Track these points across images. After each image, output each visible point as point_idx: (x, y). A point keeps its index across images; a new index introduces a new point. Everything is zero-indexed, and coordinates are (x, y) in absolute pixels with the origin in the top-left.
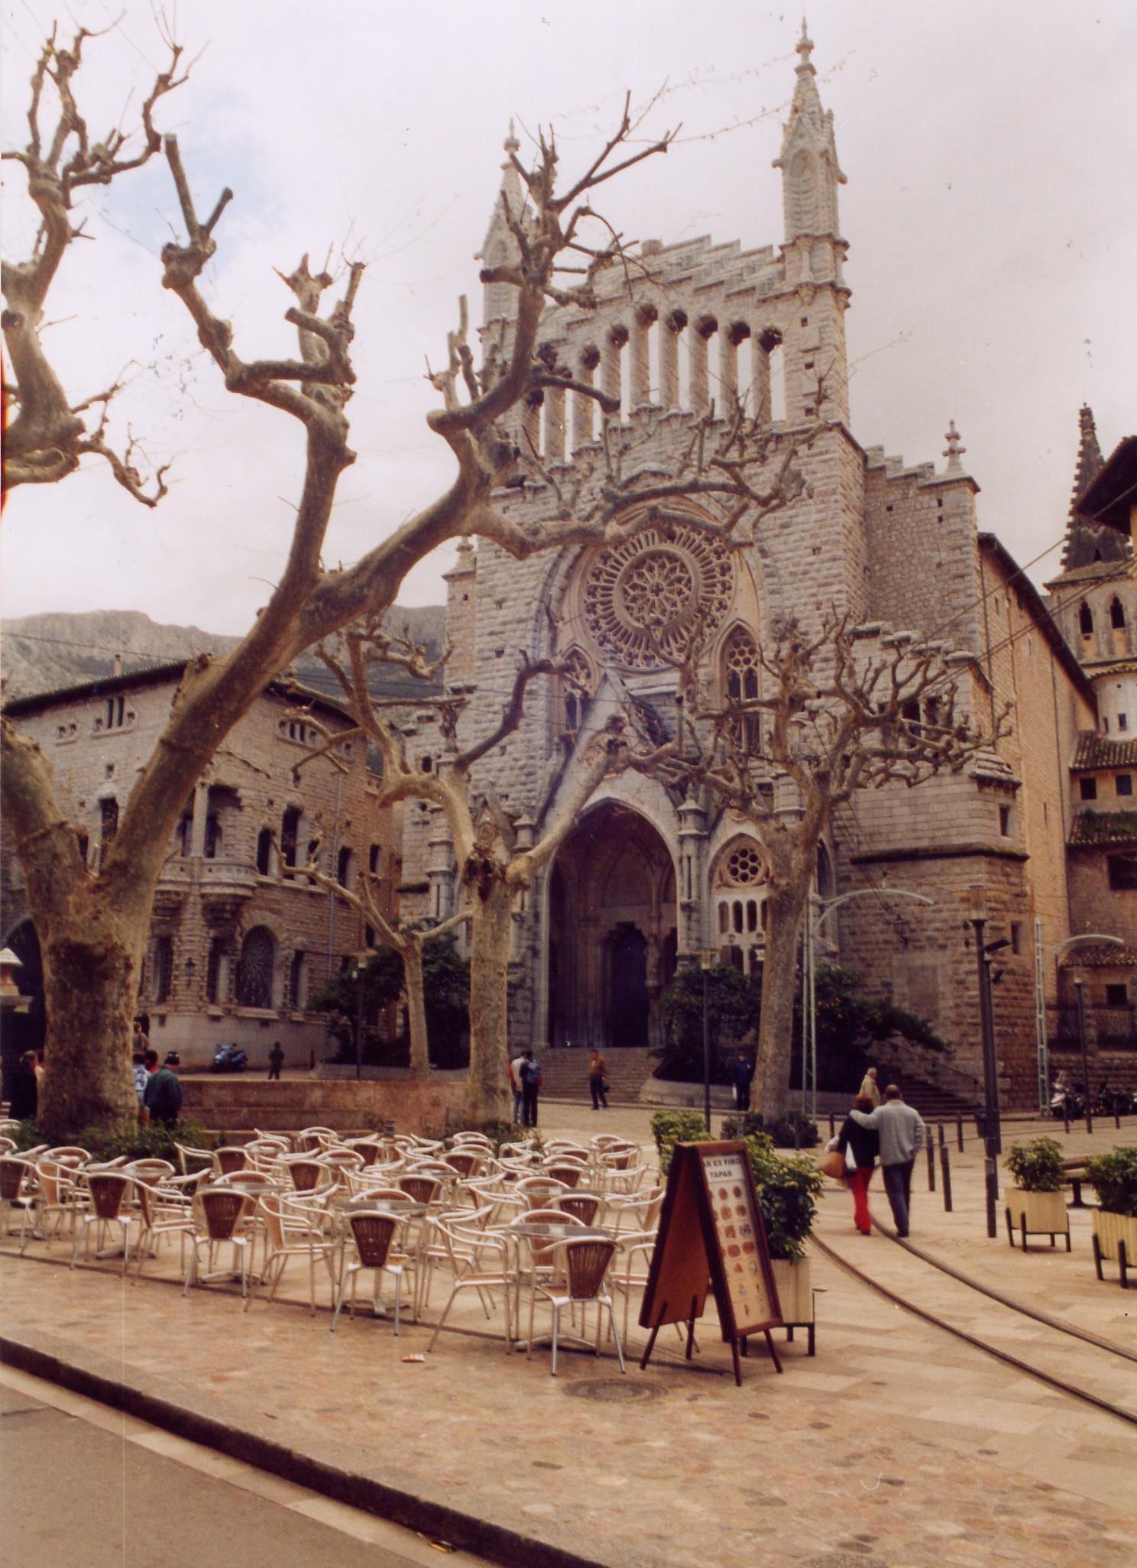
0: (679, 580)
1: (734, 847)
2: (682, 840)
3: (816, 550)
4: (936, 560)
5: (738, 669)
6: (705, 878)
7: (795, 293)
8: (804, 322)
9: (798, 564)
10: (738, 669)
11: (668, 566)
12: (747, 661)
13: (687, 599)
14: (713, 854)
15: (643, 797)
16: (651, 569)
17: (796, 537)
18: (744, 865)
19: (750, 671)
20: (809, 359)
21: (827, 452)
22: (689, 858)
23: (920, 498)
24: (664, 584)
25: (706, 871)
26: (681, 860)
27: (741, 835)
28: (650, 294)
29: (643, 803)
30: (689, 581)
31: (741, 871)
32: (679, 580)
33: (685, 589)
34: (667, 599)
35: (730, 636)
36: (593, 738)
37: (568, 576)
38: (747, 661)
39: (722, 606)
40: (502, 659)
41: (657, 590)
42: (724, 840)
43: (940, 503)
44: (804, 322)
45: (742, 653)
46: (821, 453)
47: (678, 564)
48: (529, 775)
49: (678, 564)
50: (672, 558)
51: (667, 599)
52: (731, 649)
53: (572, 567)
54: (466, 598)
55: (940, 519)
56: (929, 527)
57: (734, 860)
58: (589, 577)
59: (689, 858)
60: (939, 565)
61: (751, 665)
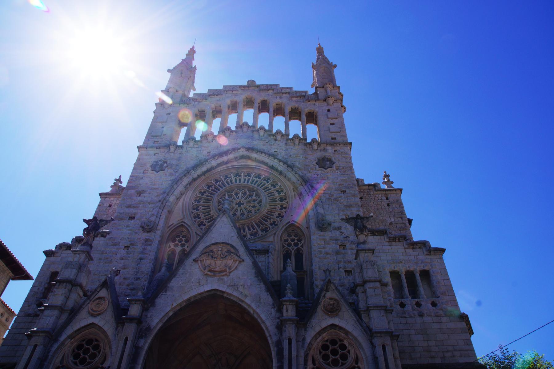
1: (325, 336)
3: (343, 192)
4: (389, 222)
5: (290, 248)
6: (302, 360)
9: (333, 195)
10: (290, 248)
11: (248, 193)
12: (296, 245)
13: (258, 210)
14: (308, 340)
16: (237, 194)
18: (335, 352)
19: (298, 250)
20: (332, 121)
22: (290, 340)
23: (377, 196)
24: (245, 202)
25: (302, 353)
26: (279, 344)
27: (333, 326)
30: (260, 201)
31: (332, 357)
32: (254, 201)
33: (257, 205)
34: (246, 209)
35: (286, 229)
36: (207, 247)
37: (186, 188)
38: (296, 245)
40: (132, 222)
41: (240, 204)
42: (318, 329)
43: (387, 199)
45: (293, 240)
48: (132, 290)
51: (246, 209)
52: (285, 237)
53: (189, 184)
54: (110, 206)
55: (388, 205)
56: (383, 207)
57: (325, 347)
58: (197, 193)
59: (290, 340)
60: (391, 224)
61: (299, 246)
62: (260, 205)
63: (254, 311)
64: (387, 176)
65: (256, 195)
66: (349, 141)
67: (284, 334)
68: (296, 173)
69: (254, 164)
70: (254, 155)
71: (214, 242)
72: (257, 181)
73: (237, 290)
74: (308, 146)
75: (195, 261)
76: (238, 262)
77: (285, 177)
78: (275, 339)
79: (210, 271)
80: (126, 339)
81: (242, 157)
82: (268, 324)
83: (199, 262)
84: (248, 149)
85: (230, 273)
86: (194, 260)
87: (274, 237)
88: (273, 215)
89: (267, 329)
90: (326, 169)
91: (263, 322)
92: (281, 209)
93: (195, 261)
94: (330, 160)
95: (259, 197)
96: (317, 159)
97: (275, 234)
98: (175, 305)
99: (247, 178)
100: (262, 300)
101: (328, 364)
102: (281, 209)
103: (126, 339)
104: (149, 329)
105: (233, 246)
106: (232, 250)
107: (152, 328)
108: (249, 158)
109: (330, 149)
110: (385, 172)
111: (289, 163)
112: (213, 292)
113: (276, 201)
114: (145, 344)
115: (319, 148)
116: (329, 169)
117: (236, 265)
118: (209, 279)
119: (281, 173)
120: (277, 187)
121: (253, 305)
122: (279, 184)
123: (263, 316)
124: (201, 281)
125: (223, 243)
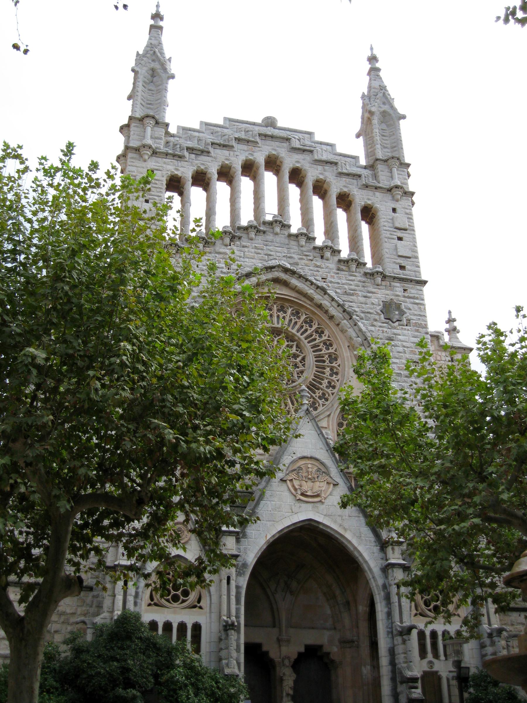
0: (295, 356)
2: (387, 568)
7: (390, 190)
8: (394, 210)
15: (346, 525)
17: (401, 349)
20: (400, 234)
21: (417, 298)
28: (281, 151)
29: (345, 530)
30: (303, 359)
32: (295, 356)
39: (330, 385)
44: (394, 210)
46: (413, 298)
47: (295, 343)
49: (295, 343)
50: (290, 338)
62: (304, 365)
63: (355, 548)
64: (451, 321)
65: (297, 346)
66: (424, 278)
67: (390, 578)
68: (355, 325)
69: (293, 294)
70: (294, 282)
71: (299, 455)
72: (296, 323)
73: (335, 522)
74: (368, 276)
75: (283, 480)
76: (332, 485)
77: (338, 325)
78: (380, 581)
79: (302, 494)
80: (229, 579)
81: (276, 281)
82: (372, 564)
83: (288, 481)
84: (286, 270)
85: (325, 498)
86: (281, 480)
87: (328, 422)
88: (321, 384)
89: (370, 569)
90: (393, 322)
91: (366, 562)
92: (331, 375)
93: (283, 480)
94: (398, 307)
95: (301, 352)
96: (382, 304)
97: (329, 416)
98: (269, 537)
99: (281, 314)
100: (363, 535)
101: (430, 610)
102: (331, 375)
103: (229, 579)
104: (245, 565)
105: (322, 463)
106: (323, 469)
107: (249, 563)
108: (286, 284)
109: (398, 287)
110: (450, 312)
111: (346, 307)
112: (307, 523)
113: (324, 361)
114: (244, 582)
115: (384, 283)
116: (397, 323)
117: (330, 489)
118: (304, 505)
119: (331, 317)
120: (324, 338)
121: (355, 542)
122: (326, 332)
123: (366, 555)
124: (293, 507)
125: (311, 458)
